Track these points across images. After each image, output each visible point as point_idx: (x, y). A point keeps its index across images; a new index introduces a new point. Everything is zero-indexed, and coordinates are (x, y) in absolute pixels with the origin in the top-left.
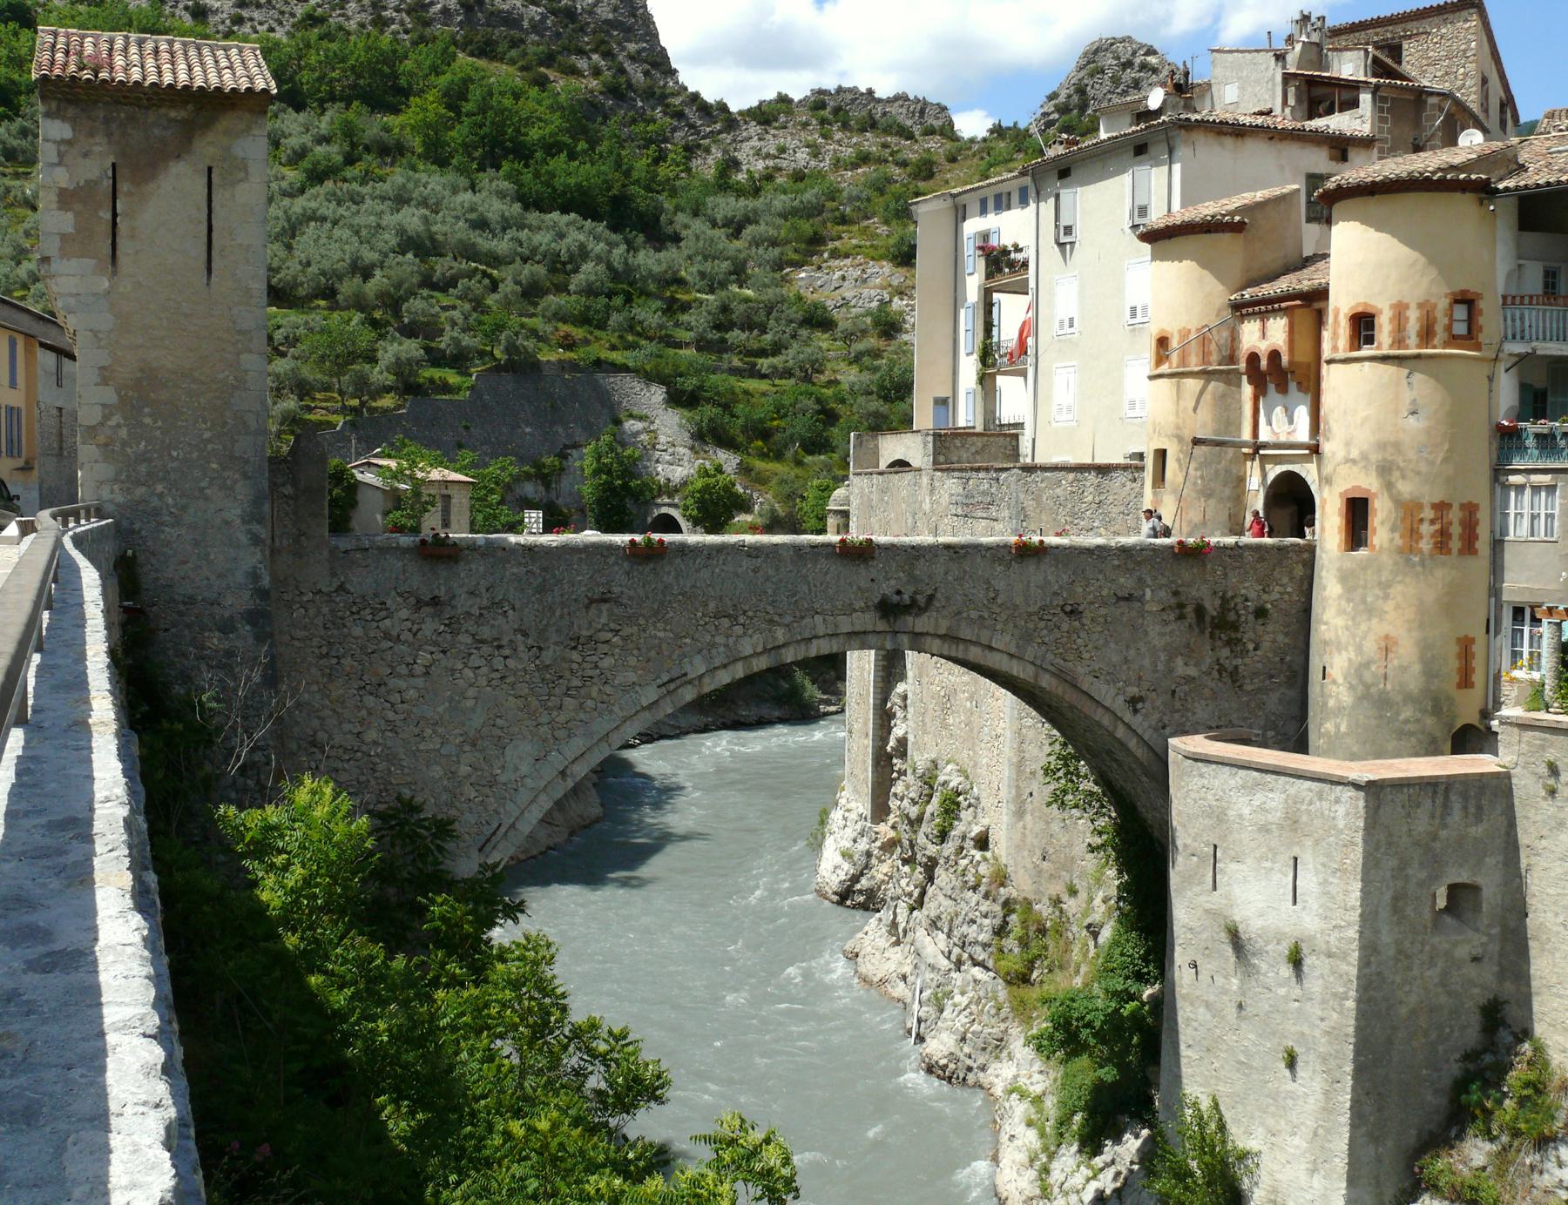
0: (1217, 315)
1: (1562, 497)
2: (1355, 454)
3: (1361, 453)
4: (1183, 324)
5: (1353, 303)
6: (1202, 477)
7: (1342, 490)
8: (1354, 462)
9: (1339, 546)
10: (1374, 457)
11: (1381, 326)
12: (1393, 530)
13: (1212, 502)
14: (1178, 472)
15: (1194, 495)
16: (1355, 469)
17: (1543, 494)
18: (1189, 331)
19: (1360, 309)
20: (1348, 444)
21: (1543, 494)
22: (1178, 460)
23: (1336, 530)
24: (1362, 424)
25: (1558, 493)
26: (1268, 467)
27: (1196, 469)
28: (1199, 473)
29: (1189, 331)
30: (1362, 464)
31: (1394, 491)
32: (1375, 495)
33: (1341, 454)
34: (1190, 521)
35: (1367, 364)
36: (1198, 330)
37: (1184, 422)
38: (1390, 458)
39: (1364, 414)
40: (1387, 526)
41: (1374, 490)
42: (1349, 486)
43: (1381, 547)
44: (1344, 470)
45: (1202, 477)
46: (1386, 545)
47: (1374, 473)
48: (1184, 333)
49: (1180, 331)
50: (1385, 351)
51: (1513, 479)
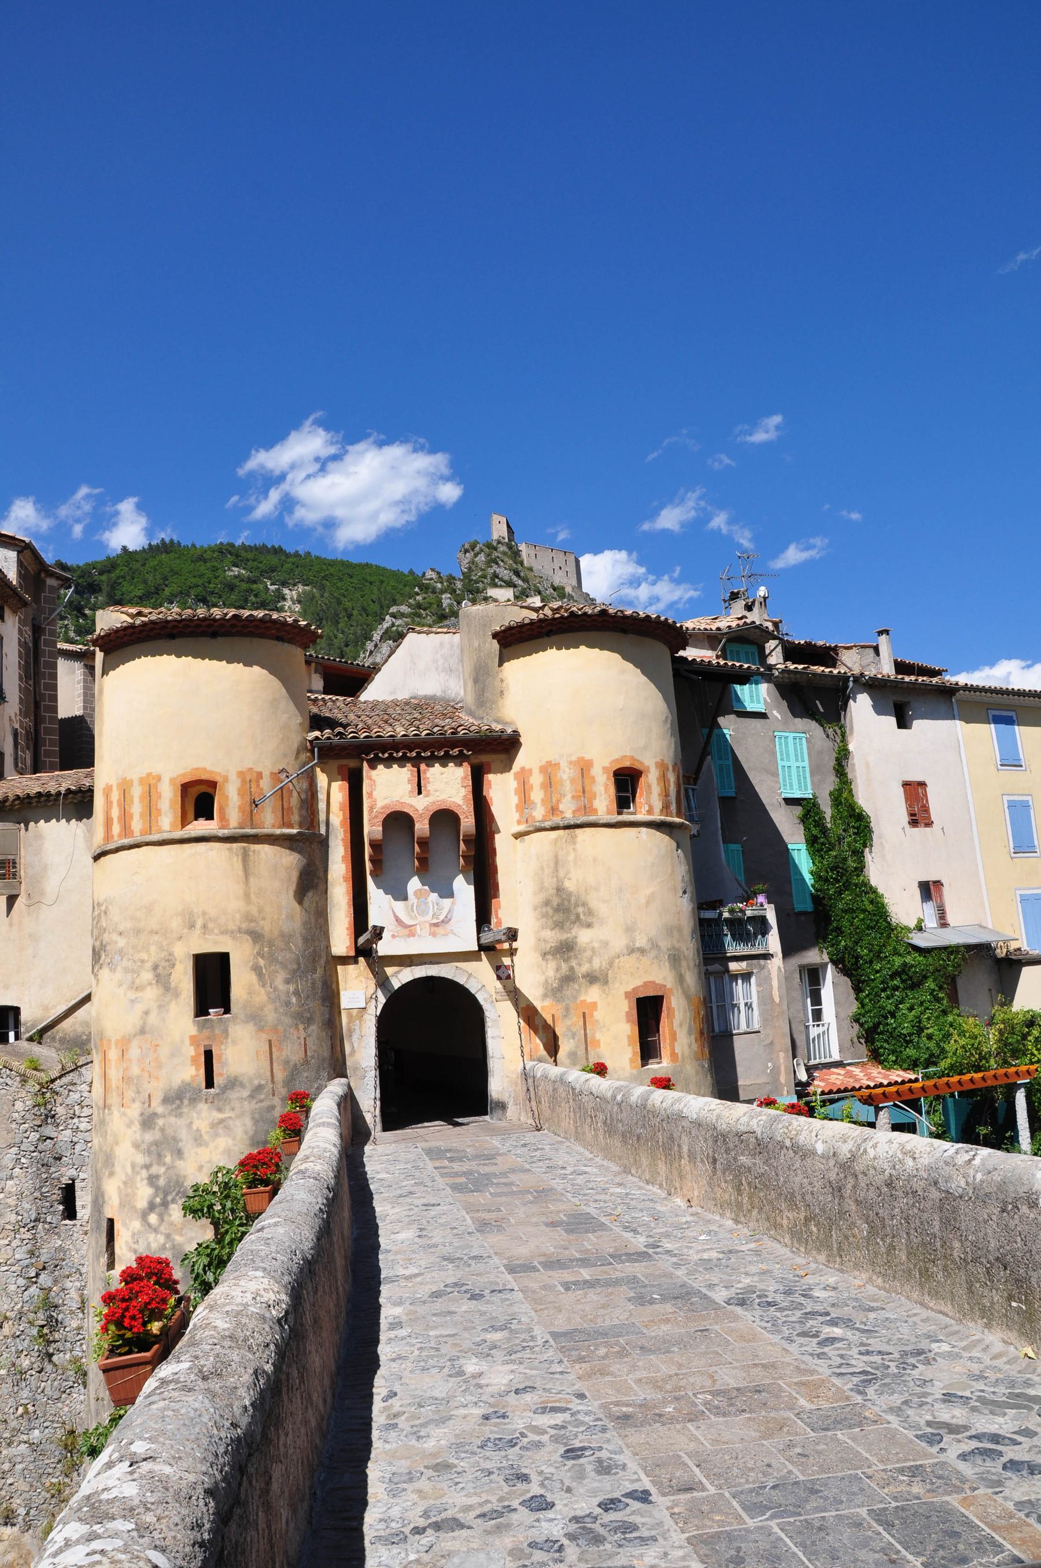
0: (297, 758)
1: (758, 985)
2: (641, 942)
3: (650, 940)
4: (248, 764)
5: (617, 756)
6: (296, 993)
7: (629, 988)
8: (642, 951)
9: (632, 1061)
10: (664, 944)
11: (649, 786)
12: (690, 1033)
13: (314, 1028)
14: (257, 987)
15: (287, 1020)
16: (645, 960)
17: (740, 982)
18: (260, 775)
19: (627, 764)
20: (629, 930)
21: (740, 982)
22: (257, 969)
23: (625, 1041)
24: (648, 903)
25: (753, 980)
26: (389, 971)
27: (287, 982)
28: (292, 988)
29: (260, 775)
30: (653, 953)
31: (685, 985)
32: (671, 990)
33: (619, 943)
34: (287, 1062)
35: (644, 830)
36: (275, 776)
37: (260, 911)
38: (677, 945)
39: (648, 891)
40: (685, 1028)
41: (669, 986)
42: (638, 983)
43: (683, 1056)
44: (628, 962)
45: (296, 993)
46: (687, 1054)
47: (667, 964)
48: (250, 779)
49: (241, 774)
50: (657, 817)
51: (733, 966)
